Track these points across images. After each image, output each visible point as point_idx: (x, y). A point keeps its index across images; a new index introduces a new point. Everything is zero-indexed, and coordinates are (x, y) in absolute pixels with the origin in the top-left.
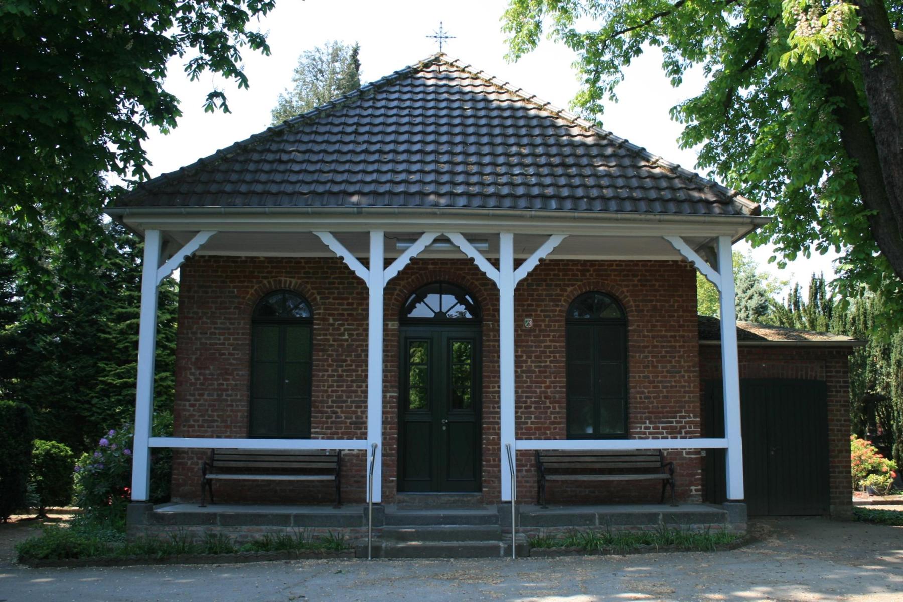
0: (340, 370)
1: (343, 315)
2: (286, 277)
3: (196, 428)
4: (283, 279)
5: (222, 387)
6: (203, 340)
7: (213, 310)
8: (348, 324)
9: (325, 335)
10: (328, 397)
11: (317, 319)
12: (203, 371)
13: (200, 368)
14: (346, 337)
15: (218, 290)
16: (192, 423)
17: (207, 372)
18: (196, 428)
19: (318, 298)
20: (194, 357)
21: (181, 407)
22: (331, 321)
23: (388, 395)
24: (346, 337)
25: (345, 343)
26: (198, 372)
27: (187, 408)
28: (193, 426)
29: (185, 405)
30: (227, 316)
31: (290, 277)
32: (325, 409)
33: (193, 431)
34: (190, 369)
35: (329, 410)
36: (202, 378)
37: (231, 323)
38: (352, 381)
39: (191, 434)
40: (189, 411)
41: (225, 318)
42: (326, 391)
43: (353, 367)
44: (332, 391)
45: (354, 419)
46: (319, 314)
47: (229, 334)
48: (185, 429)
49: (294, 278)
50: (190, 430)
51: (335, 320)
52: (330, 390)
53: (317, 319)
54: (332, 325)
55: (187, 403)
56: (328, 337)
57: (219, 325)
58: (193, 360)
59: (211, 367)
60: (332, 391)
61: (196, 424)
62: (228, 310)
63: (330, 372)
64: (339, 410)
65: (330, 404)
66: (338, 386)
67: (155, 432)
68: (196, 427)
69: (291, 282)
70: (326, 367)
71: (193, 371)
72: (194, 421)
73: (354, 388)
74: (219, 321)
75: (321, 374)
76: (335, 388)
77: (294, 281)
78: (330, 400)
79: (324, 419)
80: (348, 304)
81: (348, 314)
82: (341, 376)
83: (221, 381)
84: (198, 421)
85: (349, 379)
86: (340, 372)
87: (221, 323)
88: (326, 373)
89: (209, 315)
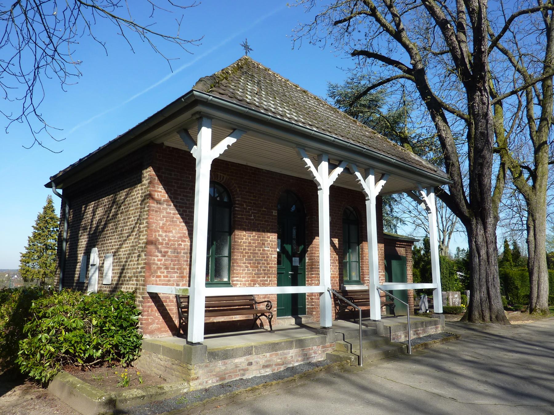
0: (249, 238)
1: (251, 203)
2: (221, 173)
3: (162, 278)
4: (219, 174)
5: (180, 246)
6: (168, 210)
7: (176, 188)
8: (254, 210)
9: (242, 215)
10: (244, 256)
11: (238, 204)
12: (167, 234)
13: (166, 232)
14: (253, 218)
15: (179, 174)
16: (159, 274)
17: (171, 235)
18: (162, 278)
19: (238, 189)
20: (161, 222)
21: (152, 262)
22: (245, 206)
23: (273, 256)
24: (253, 218)
25: (252, 222)
26: (164, 234)
27: (156, 262)
28: (159, 277)
29: (154, 260)
30: (185, 194)
31: (223, 174)
32: (242, 265)
33: (160, 280)
34: (159, 231)
35: (244, 265)
36: (167, 239)
37: (187, 200)
38: (256, 247)
39: (158, 282)
40: (157, 265)
41: (184, 196)
42: (242, 253)
43: (256, 238)
44: (246, 253)
45: (257, 271)
46: (238, 201)
47: (186, 207)
48: (153, 279)
49: (225, 174)
50: (158, 279)
51: (247, 206)
52: (244, 252)
53: (238, 204)
54: (246, 209)
55: (156, 258)
56: (244, 217)
57: (179, 200)
58: (161, 225)
59: (174, 231)
60: (246, 253)
61: (162, 275)
62: (186, 190)
63: (244, 240)
64: (249, 265)
65: (244, 261)
66: (249, 250)
67: (209, 284)
68: (162, 277)
69: (223, 177)
70: (242, 237)
71: (161, 233)
72: (161, 272)
73: (257, 251)
74: (179, 197)
75: (240, 241)
76: (247, 251)
77: (225, 176)
78: (244, 258)
79: (241, 271)
80: (254, 196)
81: (254, 203)
82: (250, 243)
83: (180, 242)
84: (164, 273)
85: (254, 245)
86: (250, 241)
87: (181, 199)
88: (242, 241)
89: (173, 192)
